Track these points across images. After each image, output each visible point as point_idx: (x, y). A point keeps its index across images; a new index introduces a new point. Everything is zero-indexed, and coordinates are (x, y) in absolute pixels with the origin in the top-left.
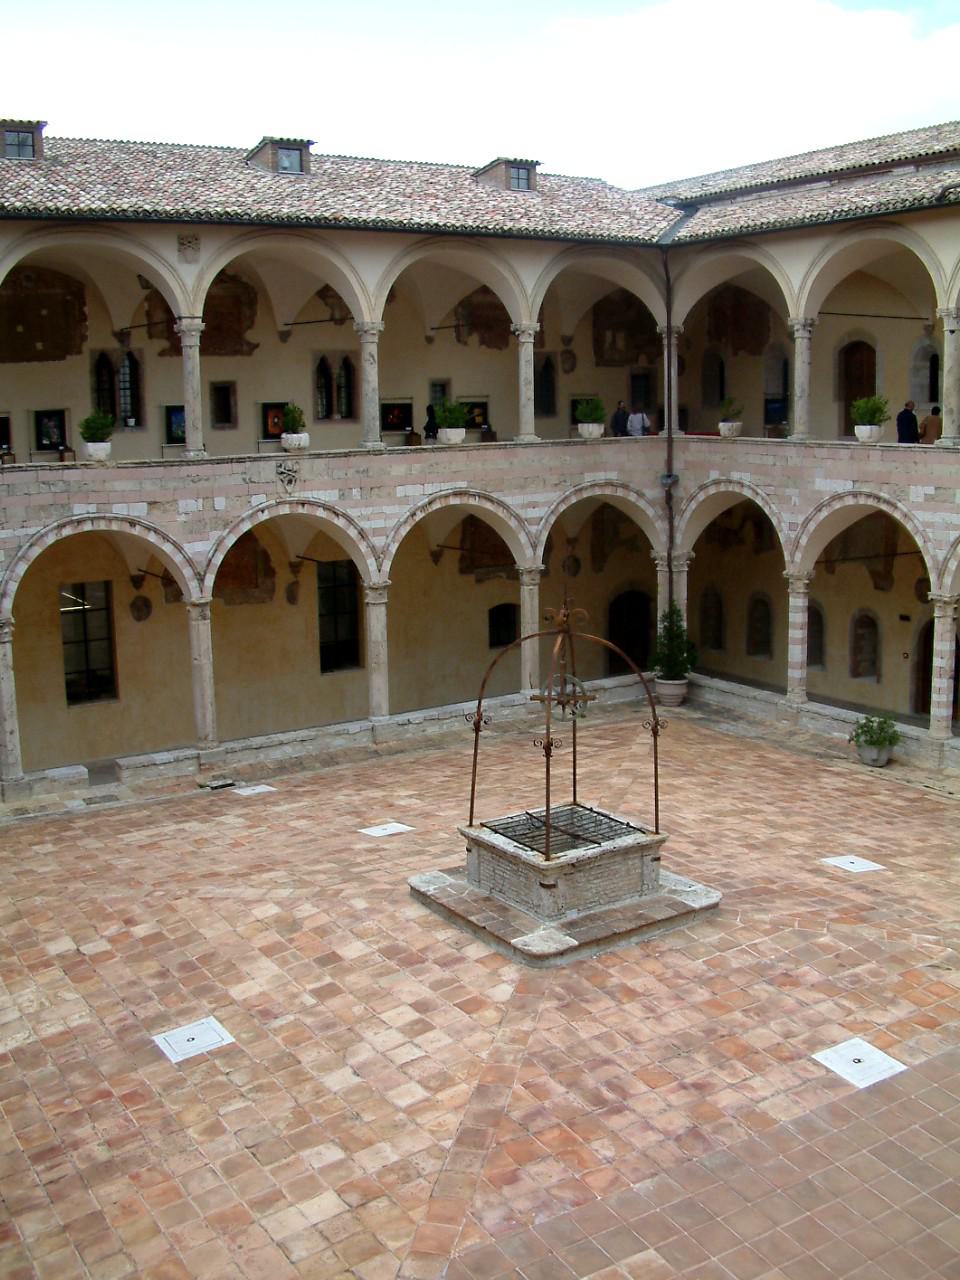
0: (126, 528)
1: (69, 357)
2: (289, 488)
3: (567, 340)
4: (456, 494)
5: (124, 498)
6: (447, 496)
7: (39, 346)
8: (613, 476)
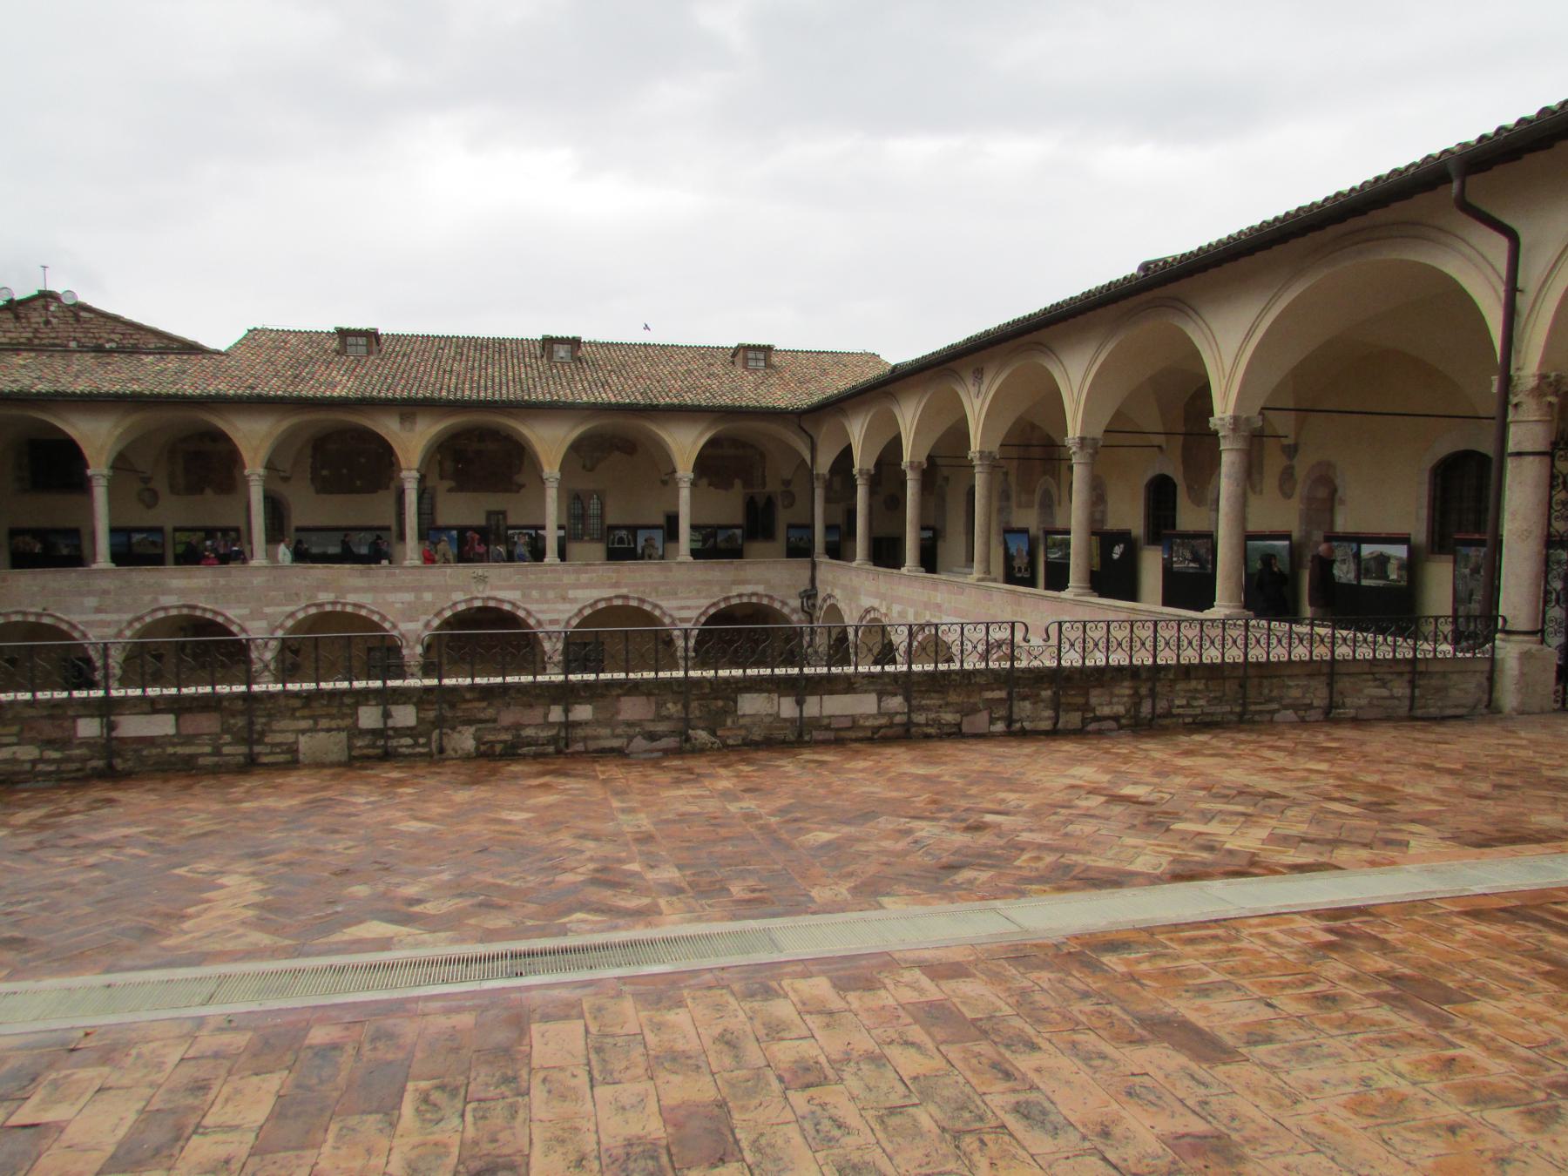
0: (357, 611)
1: (380, 492)
2: (481, 588)
3: (787, 483)
4: (617, 597)
5: (356, 590)
6: (610, 599)
7: (358, 483)
8: (760, 589)
